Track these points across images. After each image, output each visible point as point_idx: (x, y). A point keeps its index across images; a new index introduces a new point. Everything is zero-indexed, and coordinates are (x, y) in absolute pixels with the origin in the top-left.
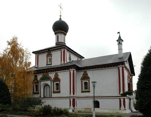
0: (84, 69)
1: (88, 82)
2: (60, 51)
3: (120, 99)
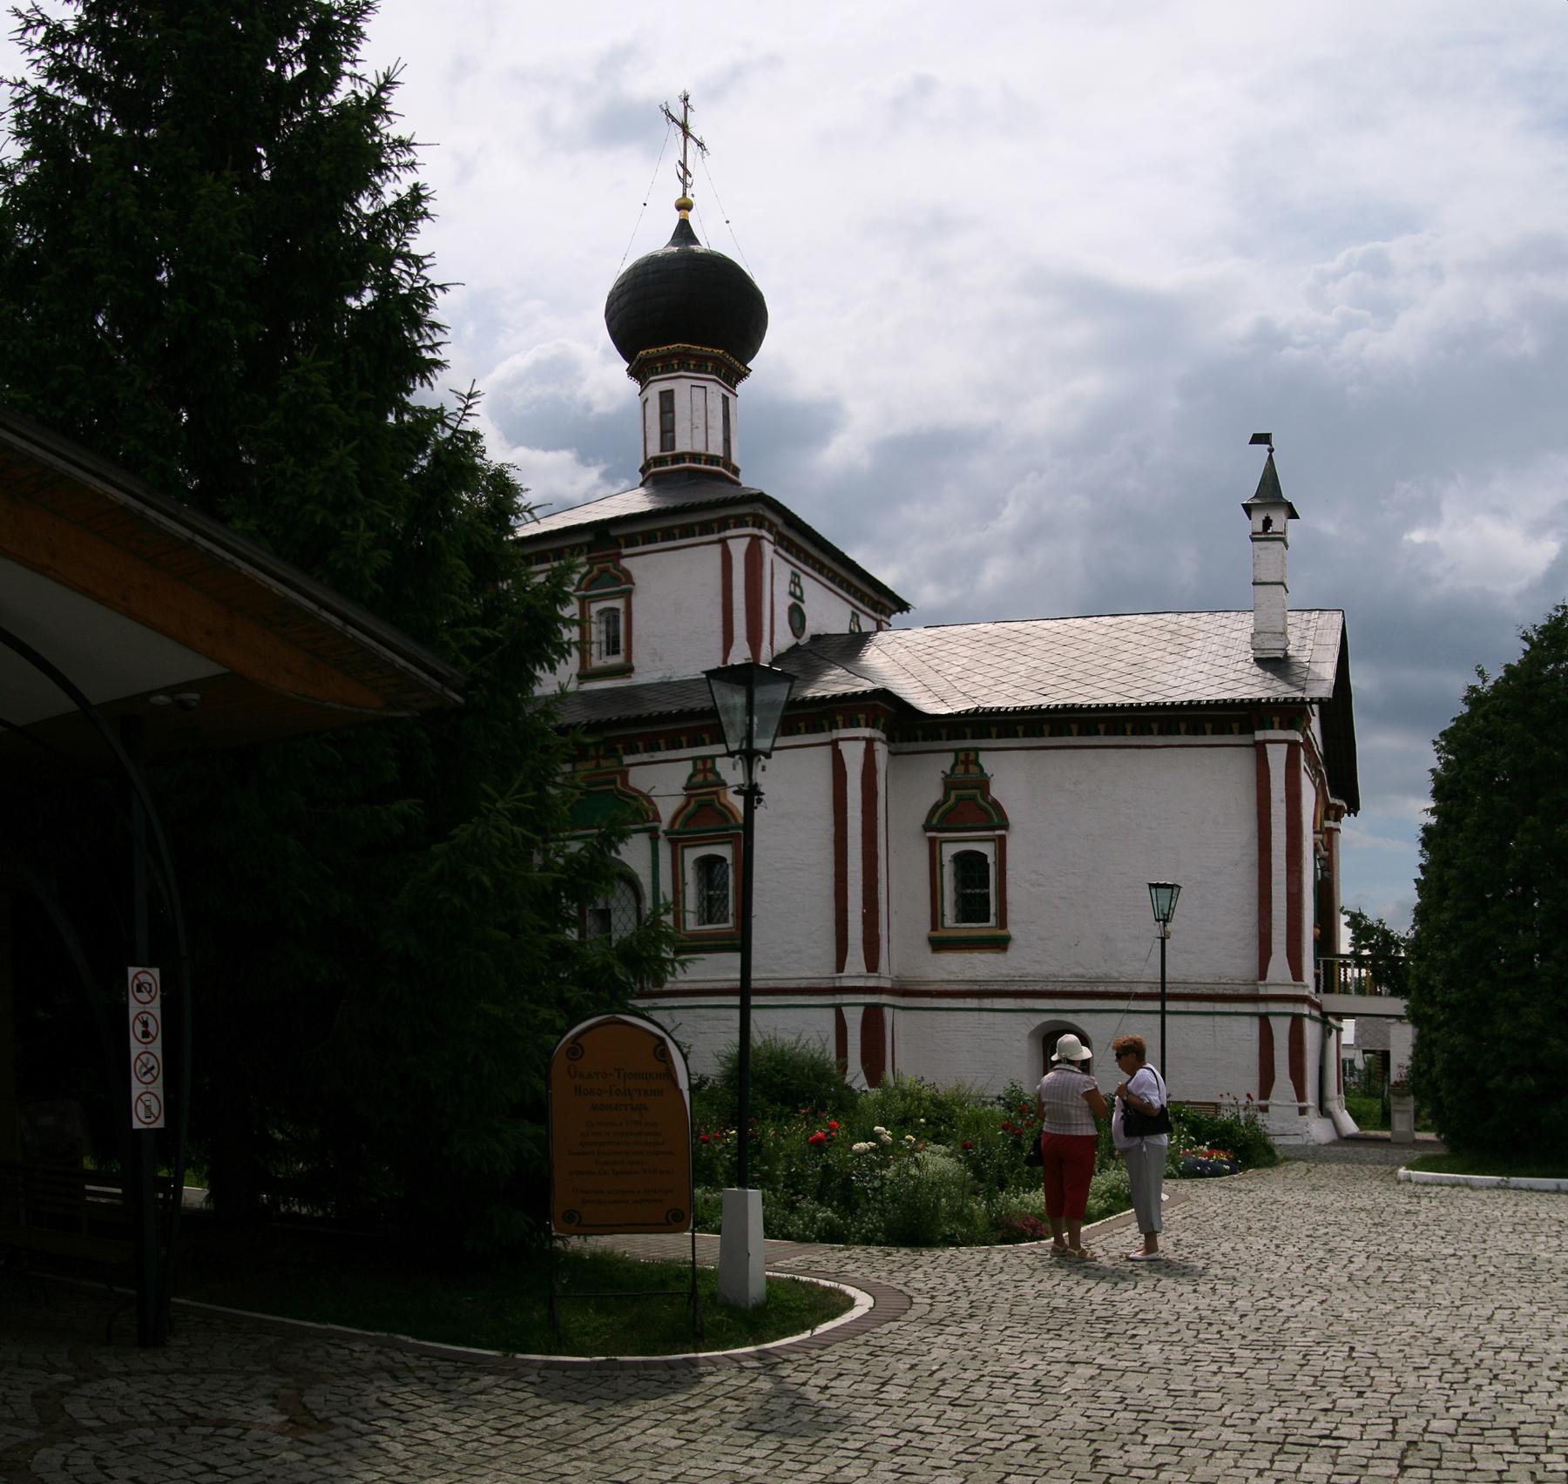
1: (988, 849)
3: (1264, 1018)
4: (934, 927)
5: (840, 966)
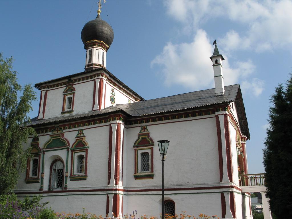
0: (142, 122)
1: (149, 151)
2: (93, 82)
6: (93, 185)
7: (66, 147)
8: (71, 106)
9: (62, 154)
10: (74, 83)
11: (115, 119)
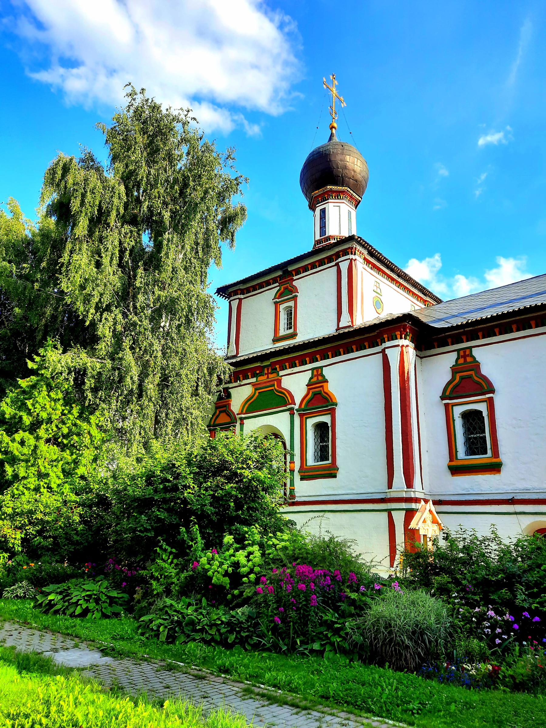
0: (457, 340)
1: (483, 407)
2: (336, 268)
4: (451, 460)
5: (390, 486)
6: (353, 489)
7: (289, 407)
8: (291, 322)
9: (280, 421)
10: (295, 278)
11: (391, 338)
